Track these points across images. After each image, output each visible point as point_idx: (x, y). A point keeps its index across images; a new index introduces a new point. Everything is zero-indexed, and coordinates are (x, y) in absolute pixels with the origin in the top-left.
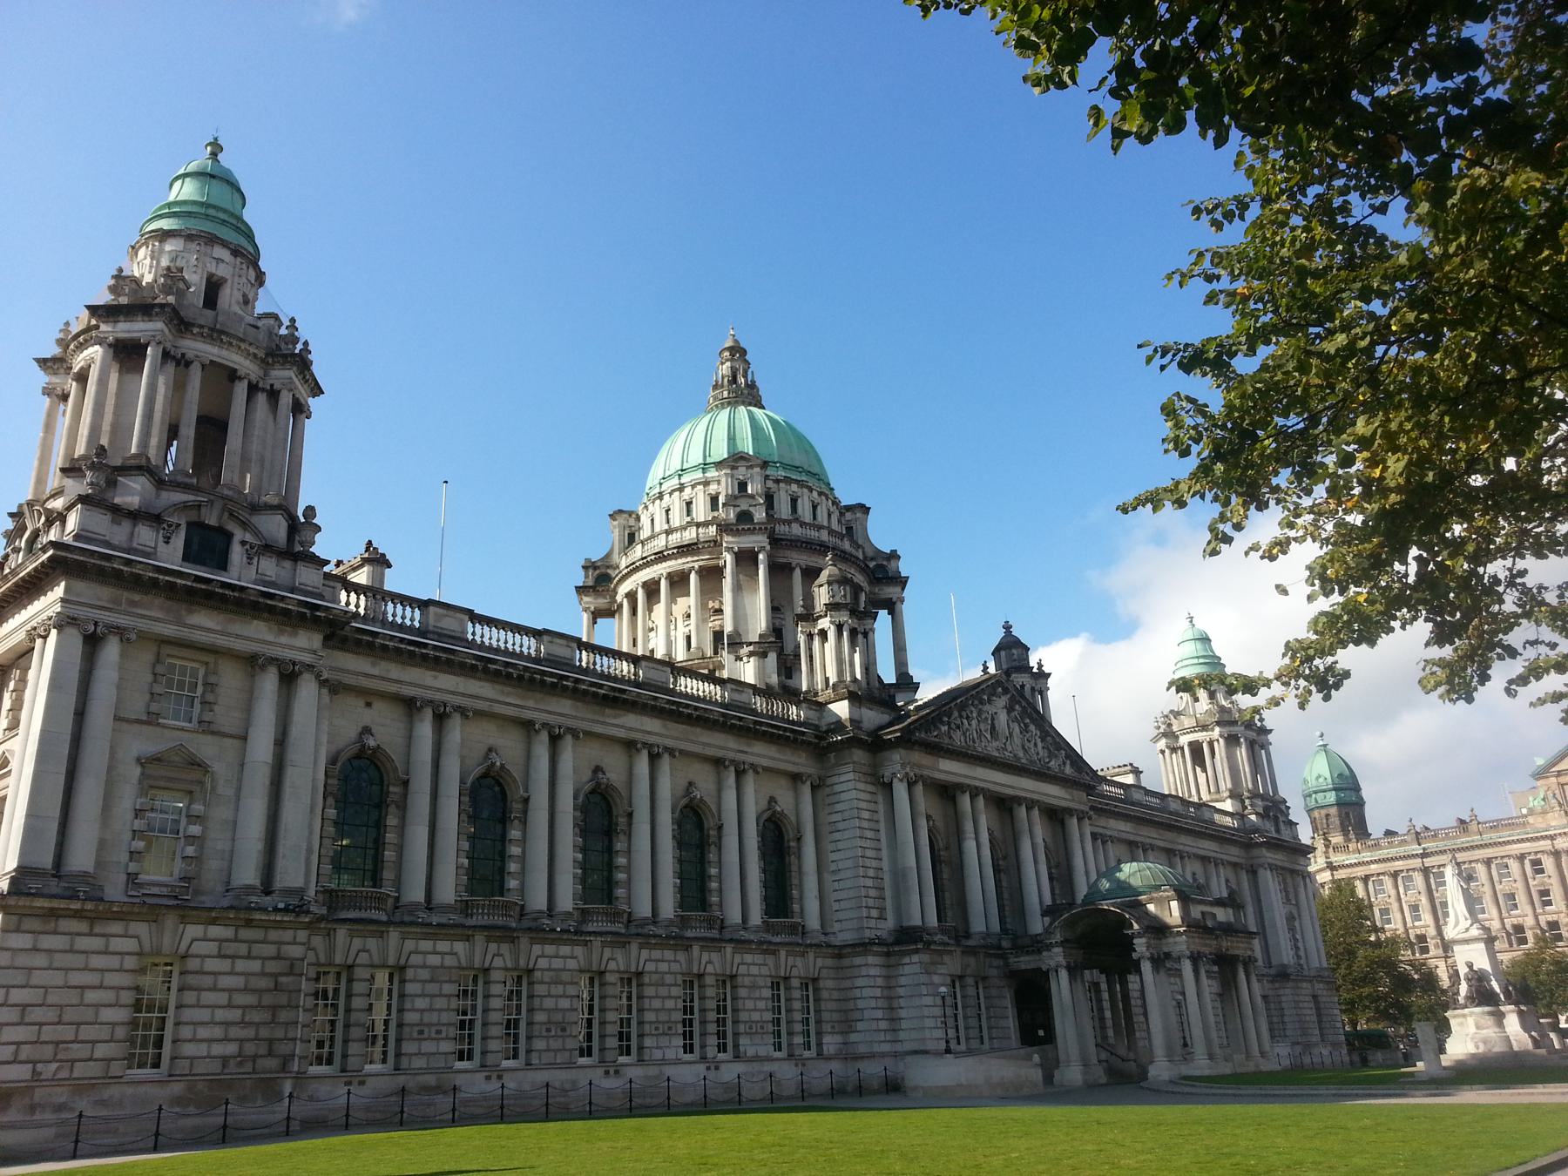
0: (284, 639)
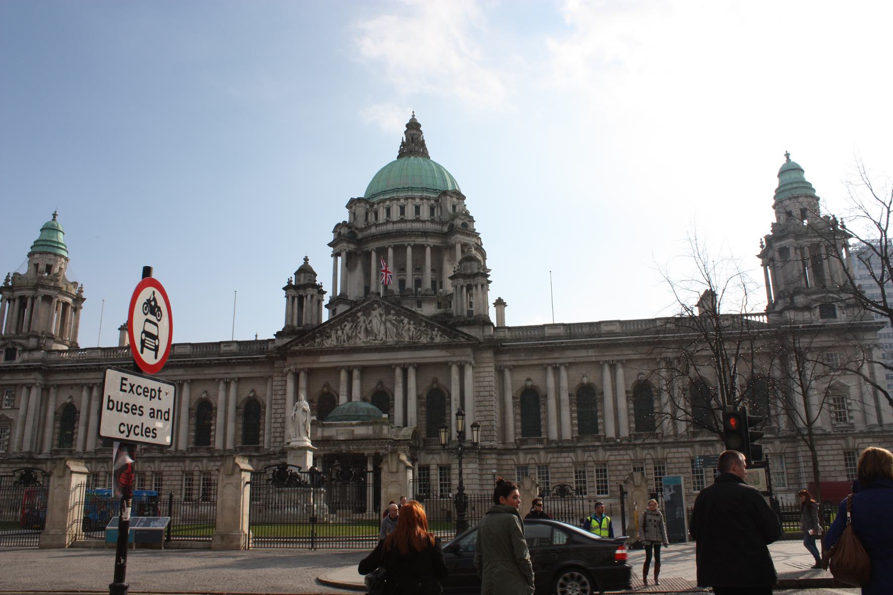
0: (28, 377)
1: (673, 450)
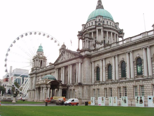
1: (128, 83)
